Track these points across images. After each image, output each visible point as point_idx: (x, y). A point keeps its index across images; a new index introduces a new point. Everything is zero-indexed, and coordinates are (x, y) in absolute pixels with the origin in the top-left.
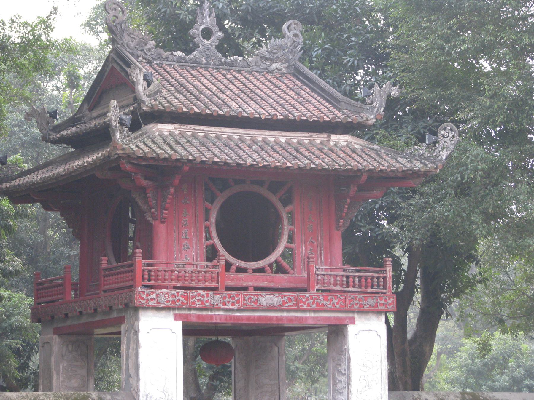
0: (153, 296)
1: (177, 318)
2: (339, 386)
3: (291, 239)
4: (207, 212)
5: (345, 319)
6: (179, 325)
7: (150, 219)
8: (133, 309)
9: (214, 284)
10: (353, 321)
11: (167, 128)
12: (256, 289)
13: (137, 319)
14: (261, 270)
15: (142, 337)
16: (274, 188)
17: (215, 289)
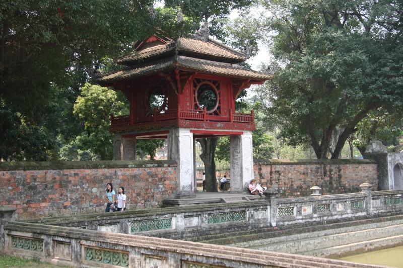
0: (184, 123)
1: (191, 131)
2: (236, 157)
3: (219, 103)
4: (194, 91)
5: (240, 132)
6: (191, 135)
7: (176, 93)
8: (176, 127)
9: (202, 119)
10: (242, 133)
11: (183, 57)
12: (210, 121)
13: (178, 132)
14: (211, 114)
15: (181, 139)
16: (214, 83)
17: (203, 120)
